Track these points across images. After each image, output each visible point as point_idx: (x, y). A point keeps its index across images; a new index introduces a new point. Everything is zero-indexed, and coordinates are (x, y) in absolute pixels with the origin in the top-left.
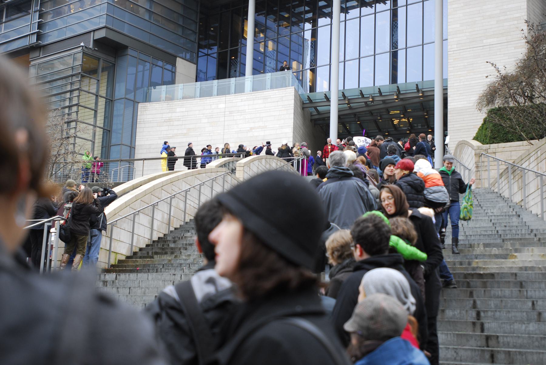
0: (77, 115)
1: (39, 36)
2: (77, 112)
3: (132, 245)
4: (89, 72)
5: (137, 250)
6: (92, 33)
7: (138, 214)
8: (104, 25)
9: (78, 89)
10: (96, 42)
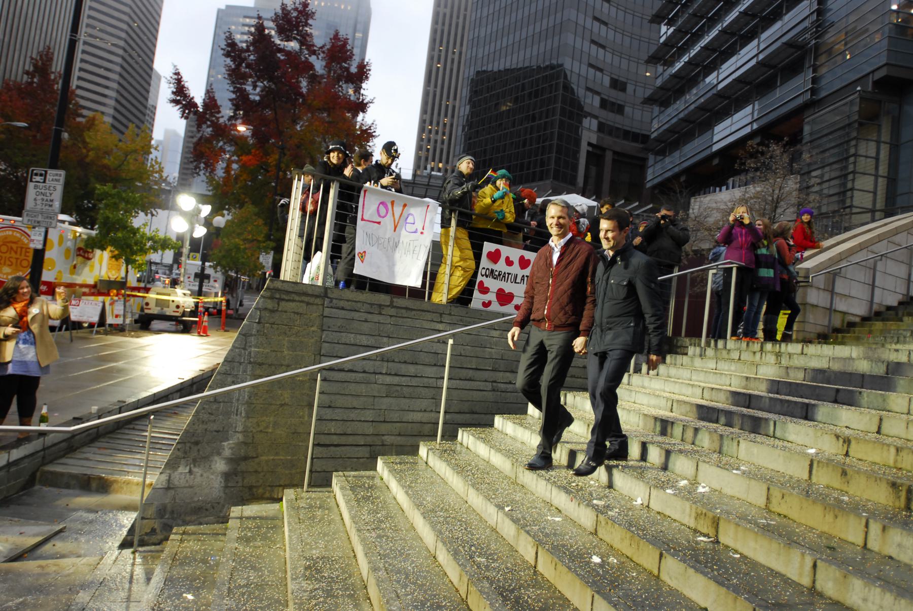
0: (855, 166)
1: (813, 91)
2: (855, 163)
3: (872, 302)
4: (868, 119)
5: (883, 309)
6: (871, 76)
7: (881, 260)
8: (884, 62)
9: (854, 138)
10: (876, 83)
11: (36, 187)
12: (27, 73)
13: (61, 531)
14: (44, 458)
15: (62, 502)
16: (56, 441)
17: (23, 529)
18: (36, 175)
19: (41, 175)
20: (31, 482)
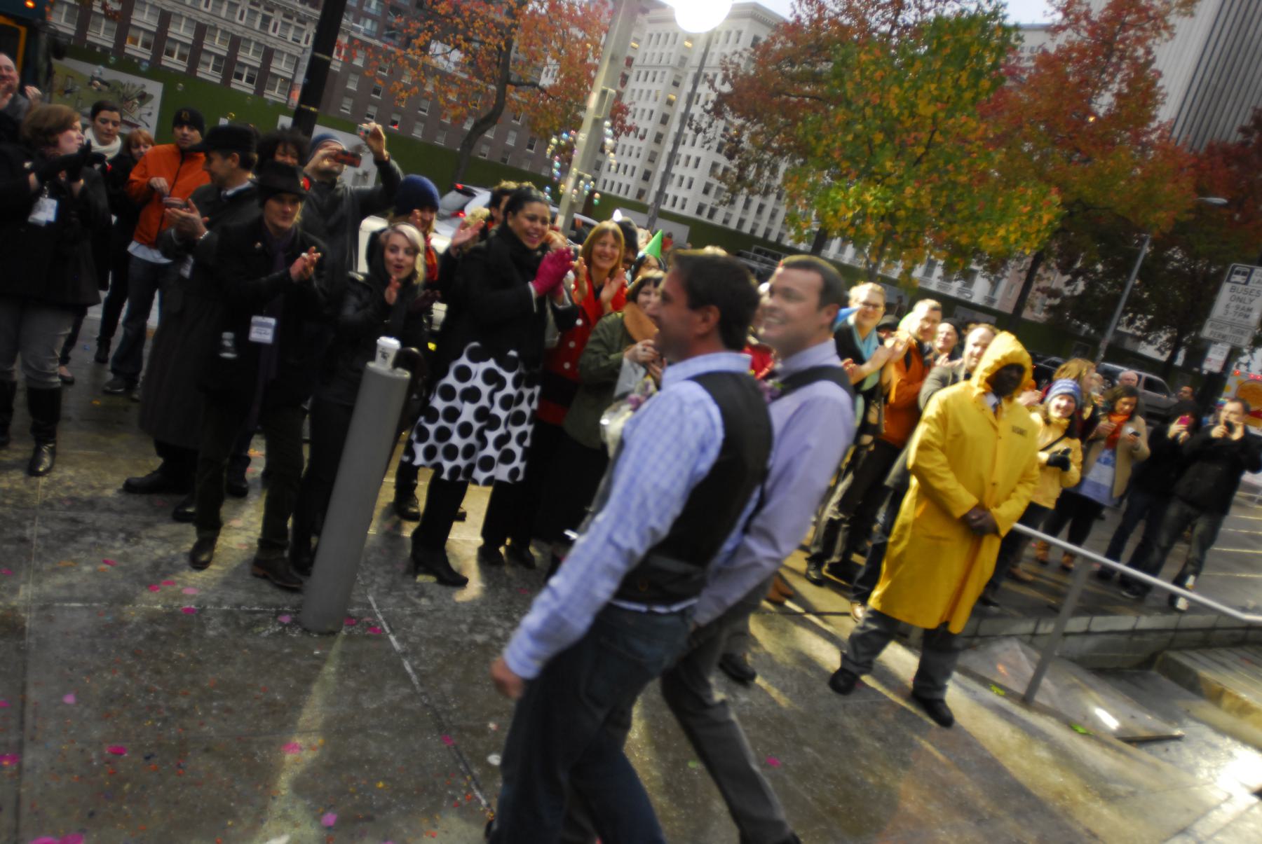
11: (1233, 290)
12: (1243, 130)
13: (1178, 738)
14: (1172, 640)
15: (1181, 704)
16: (1192, 626)
17: (1137, 713)
18: (1238, 273)
19: (1244, 274)
20: (1148, 663)
